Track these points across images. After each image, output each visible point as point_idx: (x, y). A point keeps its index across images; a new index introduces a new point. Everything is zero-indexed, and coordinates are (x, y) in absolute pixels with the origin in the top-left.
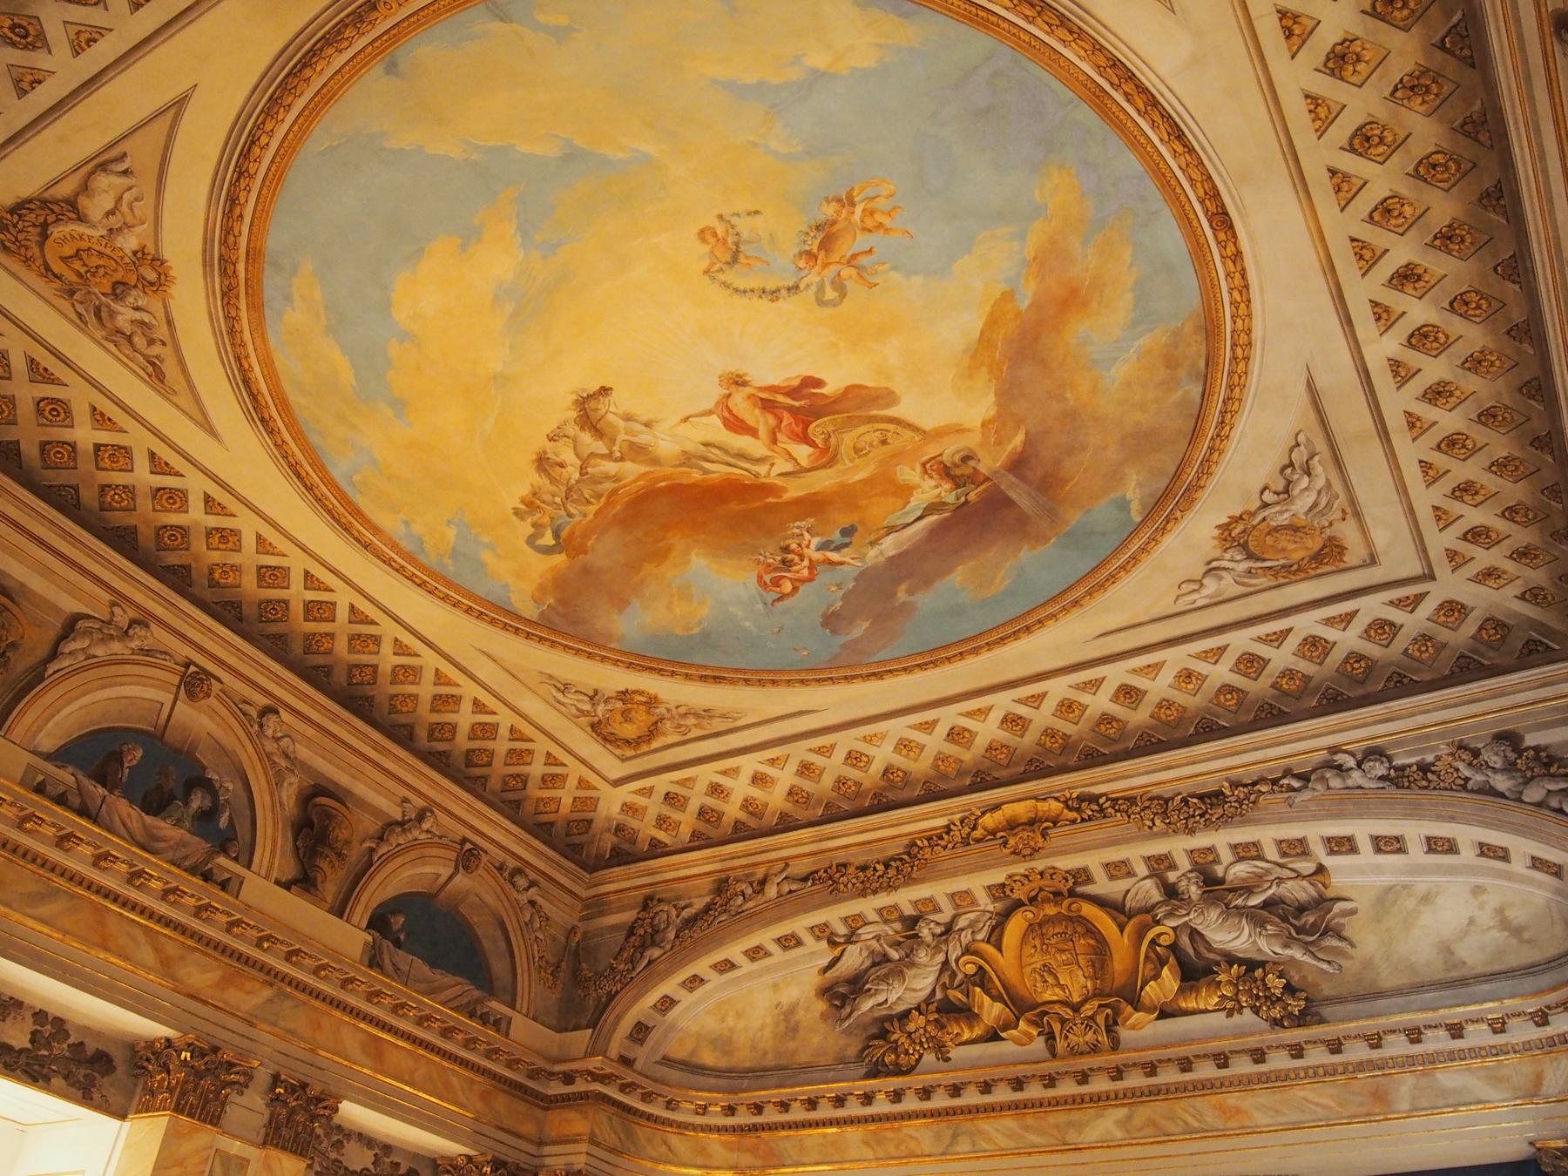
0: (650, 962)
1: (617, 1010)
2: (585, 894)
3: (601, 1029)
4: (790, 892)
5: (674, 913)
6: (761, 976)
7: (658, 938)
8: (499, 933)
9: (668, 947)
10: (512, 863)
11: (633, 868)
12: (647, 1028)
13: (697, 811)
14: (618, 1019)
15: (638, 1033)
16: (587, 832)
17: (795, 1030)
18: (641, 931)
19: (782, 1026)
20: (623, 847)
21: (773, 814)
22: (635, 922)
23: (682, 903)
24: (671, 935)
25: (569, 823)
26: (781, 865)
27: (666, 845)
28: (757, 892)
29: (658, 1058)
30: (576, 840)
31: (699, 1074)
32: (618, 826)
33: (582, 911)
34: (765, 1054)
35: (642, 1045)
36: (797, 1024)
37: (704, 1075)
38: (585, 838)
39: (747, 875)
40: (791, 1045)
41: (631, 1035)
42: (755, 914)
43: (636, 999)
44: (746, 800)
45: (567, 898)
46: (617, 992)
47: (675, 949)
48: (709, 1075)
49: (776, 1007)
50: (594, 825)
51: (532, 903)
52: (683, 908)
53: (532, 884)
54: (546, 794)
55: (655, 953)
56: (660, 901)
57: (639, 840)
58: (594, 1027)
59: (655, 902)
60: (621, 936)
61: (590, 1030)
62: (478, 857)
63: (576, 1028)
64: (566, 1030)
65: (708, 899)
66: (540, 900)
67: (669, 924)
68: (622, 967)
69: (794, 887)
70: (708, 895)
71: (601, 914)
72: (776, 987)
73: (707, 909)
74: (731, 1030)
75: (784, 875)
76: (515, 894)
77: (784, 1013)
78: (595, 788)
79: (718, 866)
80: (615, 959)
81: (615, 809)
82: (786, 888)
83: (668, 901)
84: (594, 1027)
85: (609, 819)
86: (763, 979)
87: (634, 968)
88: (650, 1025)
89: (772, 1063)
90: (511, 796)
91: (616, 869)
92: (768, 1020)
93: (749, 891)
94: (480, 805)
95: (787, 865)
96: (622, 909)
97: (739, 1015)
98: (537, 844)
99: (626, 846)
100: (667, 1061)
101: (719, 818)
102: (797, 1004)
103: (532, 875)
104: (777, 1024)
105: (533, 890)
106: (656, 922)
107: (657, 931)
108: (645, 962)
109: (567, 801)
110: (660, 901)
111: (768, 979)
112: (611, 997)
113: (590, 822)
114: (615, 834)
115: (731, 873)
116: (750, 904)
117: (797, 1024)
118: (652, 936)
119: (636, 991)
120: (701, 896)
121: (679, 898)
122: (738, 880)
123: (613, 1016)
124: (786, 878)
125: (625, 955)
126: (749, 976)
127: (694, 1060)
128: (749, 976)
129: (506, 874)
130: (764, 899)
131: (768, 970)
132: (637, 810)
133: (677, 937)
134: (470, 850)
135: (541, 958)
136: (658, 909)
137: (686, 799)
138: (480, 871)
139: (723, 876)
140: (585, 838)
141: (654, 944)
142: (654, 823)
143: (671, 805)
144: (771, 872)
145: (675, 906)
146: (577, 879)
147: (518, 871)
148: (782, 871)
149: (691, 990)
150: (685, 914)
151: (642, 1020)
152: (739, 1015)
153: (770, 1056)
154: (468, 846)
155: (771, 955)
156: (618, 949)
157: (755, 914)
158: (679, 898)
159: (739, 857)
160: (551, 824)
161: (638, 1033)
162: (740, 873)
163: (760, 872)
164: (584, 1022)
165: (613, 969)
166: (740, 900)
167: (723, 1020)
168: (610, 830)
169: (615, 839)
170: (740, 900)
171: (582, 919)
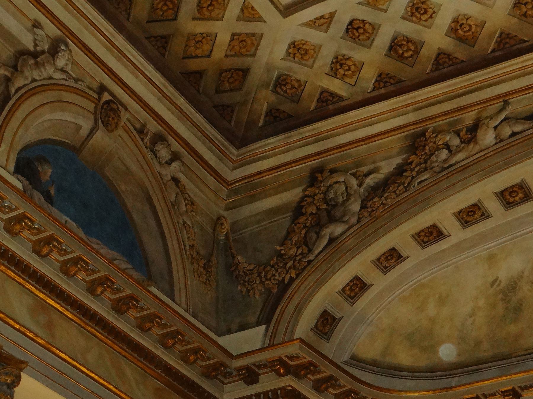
0: (332, 240)
1: (296, 300)
2: (231, 176)
3: (278, 323)
4: (514, 134)
5: (354, 182)
6: (472, 247)
7: (338, 213)
8: (147, 208)
9: (354, 220)
10: (153, 127)
11: (295, 135)
12: (334, 319)
13: (388, 44)
14: (299, 310)
15: (324, 326)
16: (240, 89)
17: (518, 310)
18: (312, 209)
19: (500, 308)
20: (282, 108)
21: (491, 36)
22: (302, 200)
23: (364, 169)
24: (356, 207)
25: (222, 72)
26: (499, 104)
27: (341, 98)
28: (469, 142)
29: (346, 357)
30: (226, 98)
31: (394, 376)
32: (279, 78)
33: (228, 197)
34: (478, 343)
35: (328, 340)
36: (521, 302)
37: (401, 377)
38: (237, 97)
39: (450, 124)
40: (513, 329)
41: (316, 326)
42: (464, 168)
43: (320, 283)
44: (456, 21)
45: (211, 180)
46: (292, 280)
47: (364, 221)
48: (406, 378)
49: (492, 284)
50: (250, 78)
51: (176, 180)
52: (367, 175)
53: (175, 157)
54: (200, 28)
55: (338, 229)
56: (333, 171)
57: (305, 95)
58: (268, 322)
59: (326, 174)
60: (285, 220)
61: (263, 328)
62: (116, 112)
63: (243, 327)
64: (229, 332)
65: (399, 160)
66: (182, 177)
67: (349, 195)
68: (293, 252)
69: (518, 128)
70: (399, 154)
71: (253, 199)
72: (491, 259)
73: (400, 171)
74: (433, 320)
75: (502, 116)
76: (157, 168)
77: (502, 292)
78: (260, 20)
79: (411, 117)
80: (282, 244)
81: (281, 50)
82: (507, 131)
83: (345, 171)
84: (268, 322)
85: (269, 68)
86: (476, 250)
87: (310, 251)
88: (337, 316)
89: (491, 353)
90: (159, 29)
91: (271, 140)
92: (481, 303)
93: (456, 142)
94: (120, 41)
95: (506, 103)
96: (282, 188)
97: (442, 301)
98: (181, 101)
99: (287, 107)
100: (356, 360)
101: (417, 52)
102: (521, 276)
103: (176, 146)
104: (493, 306)
105: (175, 165)
106: (331, 195)
107: (335, 206)
108: (325, 241)
109: (223, 38)
110: (333, 171)
111: (482, 250)
112: (284, 287)
113: (245, 72)
114: (274, 91)
115: (430, 126)
116: (460, 156)
117: (521, 302)
118: (328, 212)
119: (318, 274)
120: (390, 157)
121: (359, 164)
122: (438, 132)
123: (292, 307)
124: (506, 119)
125: (295, 239)
126: (459, 247)
127: (389, 360)
128: (459, 247)
129: (147, 139)
130: (477, 148)
131: (483, 238)
132: (307, 52)
133: (363, 207)
134: (108, 102)
135: (192, 247)
136: (331, 181)
137: (375, 28)
138: (120, 131)
139: (418, 129)
140: (237, 97)
141: (332, 220)
142: (327, 69)
143: (354, 39)
144: (485, 114)
145: (354, 175)
146: (223, 155)
147: (158, 138)
148: (500, 111)
149: (385, 270)
150: (370, 181)
151: (330, 309)
152: (442, 301)
153: (486, 345)
154: (106, 97)
155: (489, 216)
156: (284, 233)
157: (464, 168)
158: (359, 164)
159: (440, 102)
160: (200, 74)
161: (324, 326)
162: (441, 122)
163: (469, 118)
164: (253, 319)
165: (280, 255)
166: (444, 154)
167: (421, 309)
168: (267, 86)
169: (272, 98)
170: (444, 154)
171: (228, 208)
